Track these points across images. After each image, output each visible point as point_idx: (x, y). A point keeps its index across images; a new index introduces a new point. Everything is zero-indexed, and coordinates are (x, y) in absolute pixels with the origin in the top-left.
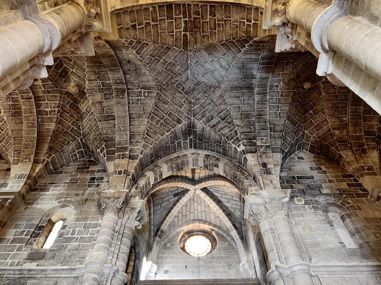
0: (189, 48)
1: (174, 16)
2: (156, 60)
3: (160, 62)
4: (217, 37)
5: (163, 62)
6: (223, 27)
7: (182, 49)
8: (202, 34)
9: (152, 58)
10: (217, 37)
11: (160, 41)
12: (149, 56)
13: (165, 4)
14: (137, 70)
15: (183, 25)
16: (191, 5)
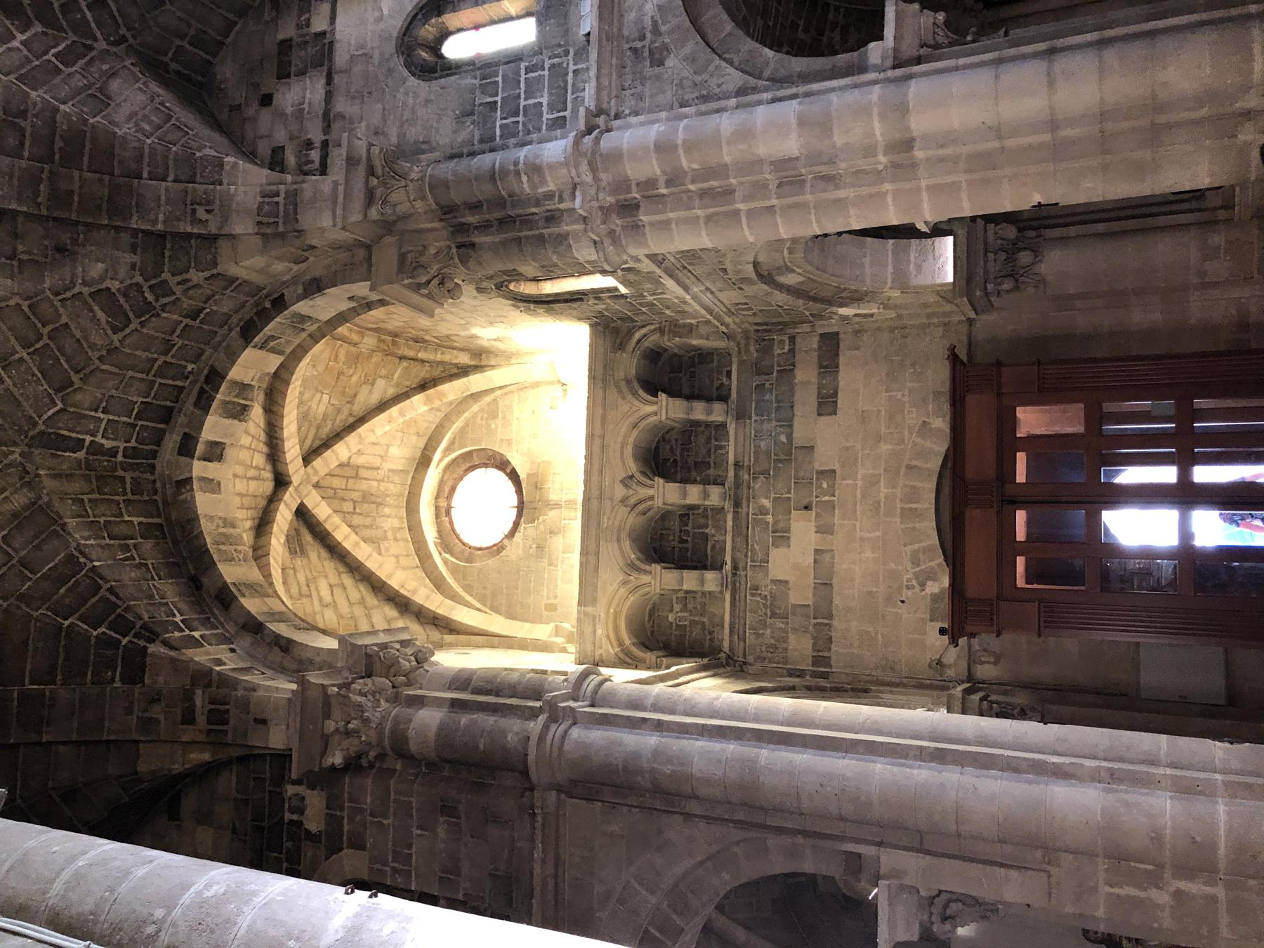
0: (37, 452)
1: (140, 423)
2: (32, 337)
3: (18, 348)
4: (92, 542)
5: (17, 356)
6: (126, 559)
7: (41, 427)
8: (85, 497)
9: (49, 328)
10: (92, 542)
11: (104, 367)
12: (64, 319)
13: (177, 405)
14: (15, 263)
15: (108, 444)
16: (152, 473)
